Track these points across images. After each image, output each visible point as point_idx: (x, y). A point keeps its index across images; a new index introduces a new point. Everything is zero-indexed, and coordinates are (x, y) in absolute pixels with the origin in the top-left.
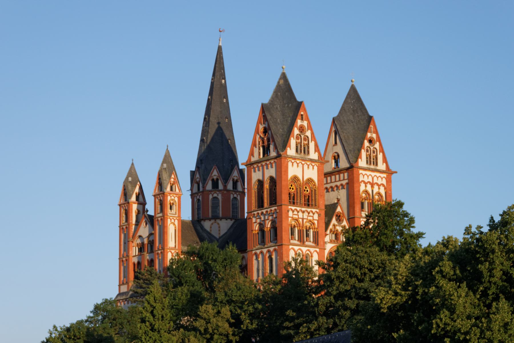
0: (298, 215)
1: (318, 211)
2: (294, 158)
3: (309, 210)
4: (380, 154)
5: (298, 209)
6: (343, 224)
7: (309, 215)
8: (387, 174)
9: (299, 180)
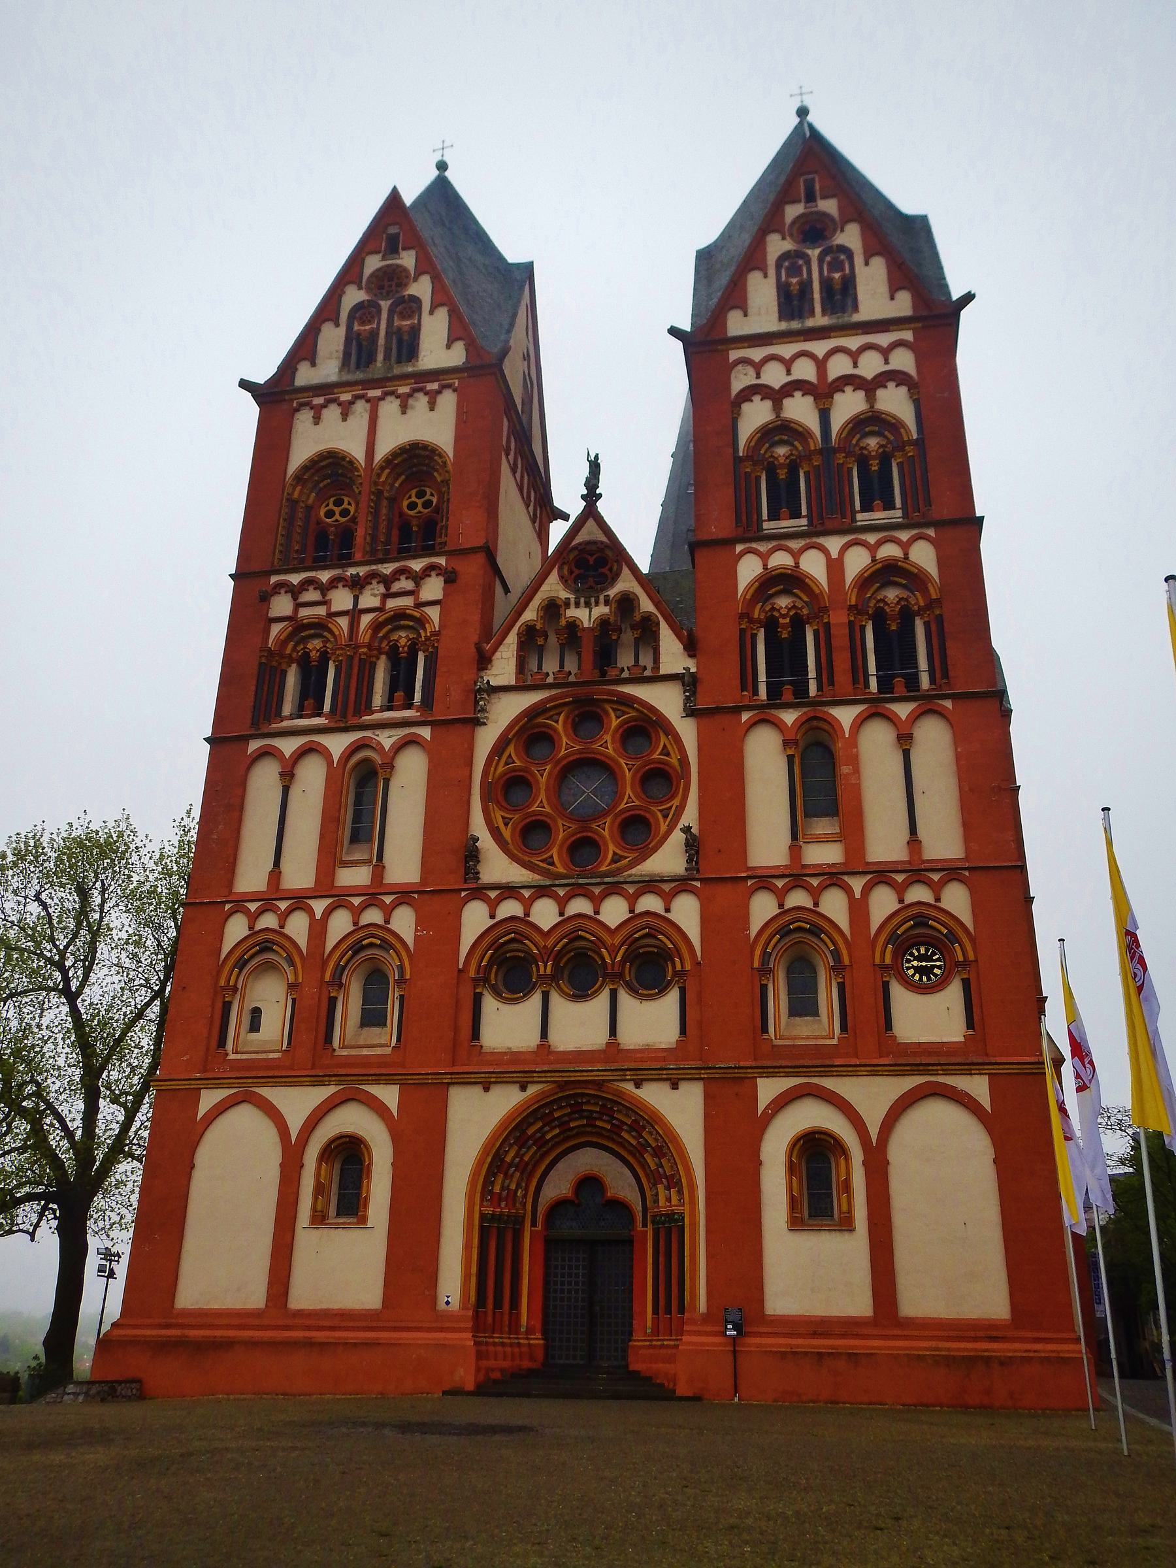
0: (325, 603)
1: (442, 561)
2: (324, 389)
3: (388, 569)
4: (867, 264)
5: (324, 576)
6: (612, 592)
7: (396, 587)
8: (920, 325)
9: (352, 462)
